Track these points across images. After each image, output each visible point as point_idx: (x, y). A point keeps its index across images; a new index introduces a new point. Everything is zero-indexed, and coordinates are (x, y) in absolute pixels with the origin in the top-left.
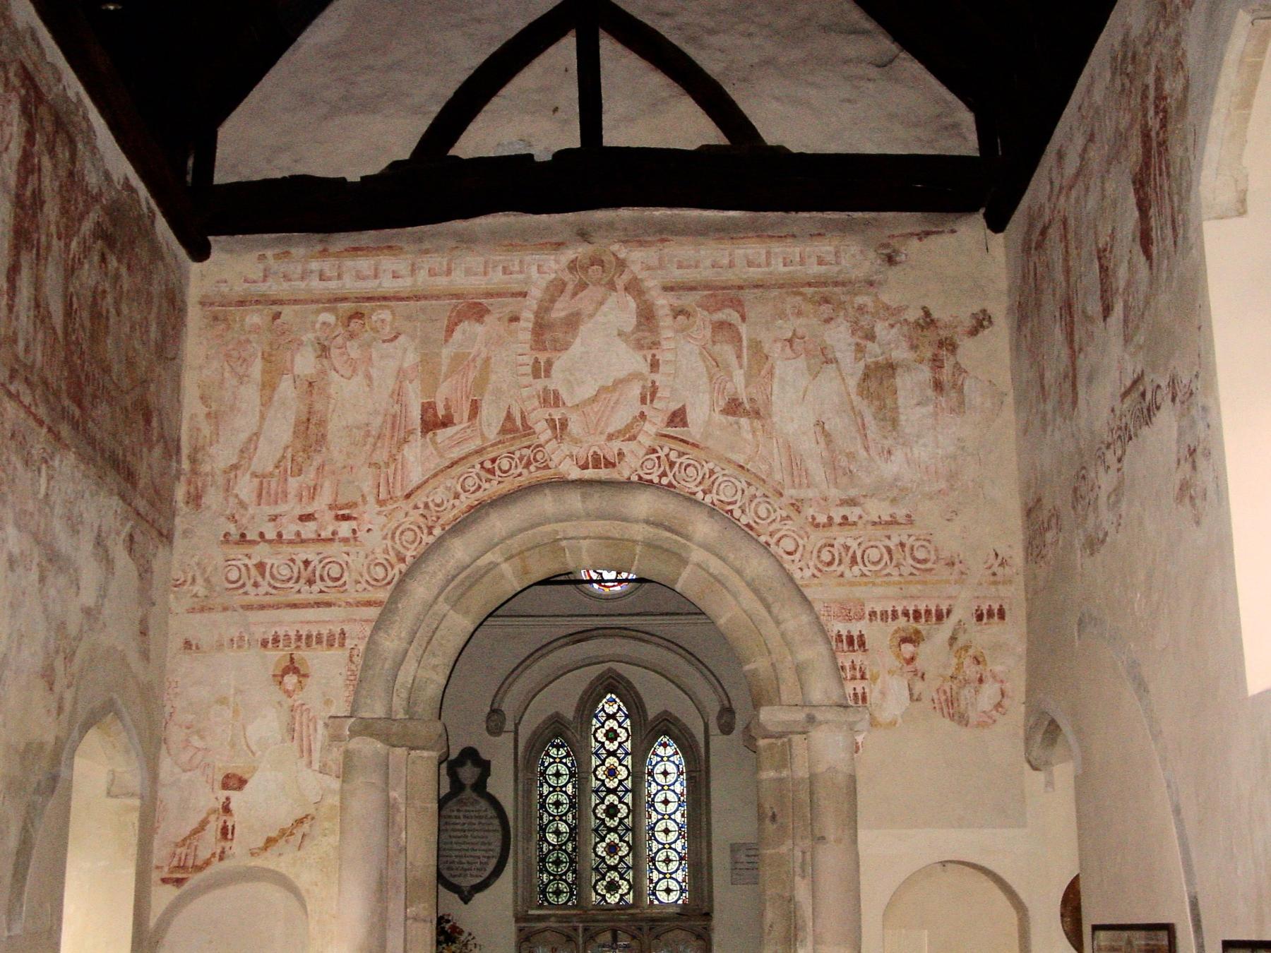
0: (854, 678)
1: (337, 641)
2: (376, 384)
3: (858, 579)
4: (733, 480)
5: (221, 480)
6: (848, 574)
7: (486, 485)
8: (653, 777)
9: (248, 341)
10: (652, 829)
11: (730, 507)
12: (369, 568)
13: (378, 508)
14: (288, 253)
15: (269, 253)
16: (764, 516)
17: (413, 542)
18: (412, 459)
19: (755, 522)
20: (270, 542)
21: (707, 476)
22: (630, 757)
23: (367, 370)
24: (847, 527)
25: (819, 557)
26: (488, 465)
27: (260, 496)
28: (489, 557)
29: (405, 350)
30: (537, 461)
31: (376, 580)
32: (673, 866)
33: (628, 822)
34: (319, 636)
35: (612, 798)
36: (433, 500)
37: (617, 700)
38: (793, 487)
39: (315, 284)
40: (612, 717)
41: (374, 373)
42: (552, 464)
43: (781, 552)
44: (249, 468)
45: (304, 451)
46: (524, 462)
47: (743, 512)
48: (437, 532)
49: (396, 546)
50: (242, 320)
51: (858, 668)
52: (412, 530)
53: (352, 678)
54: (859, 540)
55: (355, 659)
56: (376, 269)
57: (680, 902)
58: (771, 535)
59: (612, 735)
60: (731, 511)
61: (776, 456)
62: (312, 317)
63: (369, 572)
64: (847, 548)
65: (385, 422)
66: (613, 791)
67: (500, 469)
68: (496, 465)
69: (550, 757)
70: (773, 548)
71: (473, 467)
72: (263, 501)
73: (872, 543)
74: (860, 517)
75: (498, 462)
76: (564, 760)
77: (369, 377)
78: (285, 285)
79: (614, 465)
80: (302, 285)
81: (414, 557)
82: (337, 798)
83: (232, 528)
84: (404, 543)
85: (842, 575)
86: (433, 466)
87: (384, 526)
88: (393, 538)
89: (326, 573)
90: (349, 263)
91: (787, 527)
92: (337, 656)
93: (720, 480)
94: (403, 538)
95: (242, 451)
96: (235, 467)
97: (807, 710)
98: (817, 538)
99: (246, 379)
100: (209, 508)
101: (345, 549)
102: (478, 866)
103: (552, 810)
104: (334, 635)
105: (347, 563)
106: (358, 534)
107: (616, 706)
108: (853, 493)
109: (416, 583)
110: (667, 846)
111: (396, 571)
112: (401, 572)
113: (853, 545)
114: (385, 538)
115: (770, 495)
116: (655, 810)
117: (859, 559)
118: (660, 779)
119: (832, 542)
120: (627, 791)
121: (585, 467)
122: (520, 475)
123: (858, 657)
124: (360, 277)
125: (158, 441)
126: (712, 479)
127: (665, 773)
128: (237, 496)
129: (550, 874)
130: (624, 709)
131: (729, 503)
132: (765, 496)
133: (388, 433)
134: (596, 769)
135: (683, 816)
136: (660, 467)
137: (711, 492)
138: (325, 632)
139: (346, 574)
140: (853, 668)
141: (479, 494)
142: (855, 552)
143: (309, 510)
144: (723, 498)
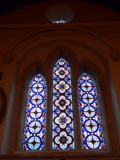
8: (81, 88)
10: (83, 110)
22: (70, 81)
32: (95, 128)
35: (62, 97)
40: (63, 66)
59: (62, 73)
66: (63, 94)
69: (36, 81)
76: (41, 82)
107: (64, 63)
118: (84, 89)
127: (87, 87)
129: (31, 133)
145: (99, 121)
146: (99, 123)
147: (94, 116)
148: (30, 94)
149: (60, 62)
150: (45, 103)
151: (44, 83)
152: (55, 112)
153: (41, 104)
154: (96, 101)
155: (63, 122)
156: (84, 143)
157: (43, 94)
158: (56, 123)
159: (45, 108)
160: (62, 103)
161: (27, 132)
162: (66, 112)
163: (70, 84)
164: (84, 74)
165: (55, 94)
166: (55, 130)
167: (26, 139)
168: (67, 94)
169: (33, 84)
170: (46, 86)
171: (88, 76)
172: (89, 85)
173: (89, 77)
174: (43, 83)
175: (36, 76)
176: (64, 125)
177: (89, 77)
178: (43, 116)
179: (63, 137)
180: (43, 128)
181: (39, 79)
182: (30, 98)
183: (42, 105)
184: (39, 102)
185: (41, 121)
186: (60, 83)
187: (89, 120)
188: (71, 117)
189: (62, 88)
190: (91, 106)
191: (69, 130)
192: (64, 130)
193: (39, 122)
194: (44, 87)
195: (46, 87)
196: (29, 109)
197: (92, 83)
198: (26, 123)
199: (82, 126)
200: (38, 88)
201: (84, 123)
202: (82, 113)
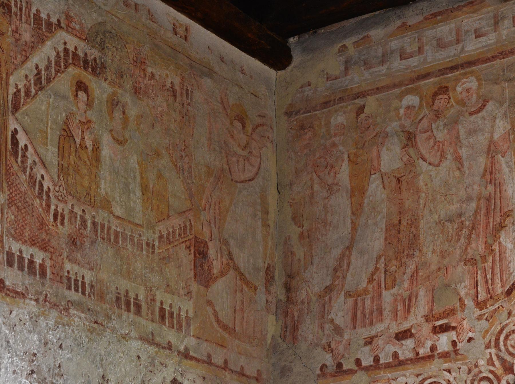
2: (466, 164)
5: (316, 307)
9: (334, 145)
13: (477, 312)
14: (367, 37)
15: (349, 42)
20: (367, 369)
23: (456, 151)
27: (354, 317)
29: (494, 119)
39: (397, 64)
41: (464, 152)
44: (343, 287)
45: (397, 258)
49: (501, 354)
50: (328, 124)
56: (457, 34)
62: (395, 103)
65: (478, 208)
72: (358, 323)
77: (458, 159)
78: (367, 74)
80: (383, 69)
83: (329, 360)
84: (511, 349)
87: (487, 332)
90: (430, 33)
94: (509, 342)
95: (335, 270)
96: (329, 289)
99: (335, 188)
100: (306, 339)
101: (446, 366)
106: (459, 345)
114: (488, 347)
124: (441, 45)
125: (223, 274)
128: (332, 320)
133: (482, 218)
143: (406, 326)
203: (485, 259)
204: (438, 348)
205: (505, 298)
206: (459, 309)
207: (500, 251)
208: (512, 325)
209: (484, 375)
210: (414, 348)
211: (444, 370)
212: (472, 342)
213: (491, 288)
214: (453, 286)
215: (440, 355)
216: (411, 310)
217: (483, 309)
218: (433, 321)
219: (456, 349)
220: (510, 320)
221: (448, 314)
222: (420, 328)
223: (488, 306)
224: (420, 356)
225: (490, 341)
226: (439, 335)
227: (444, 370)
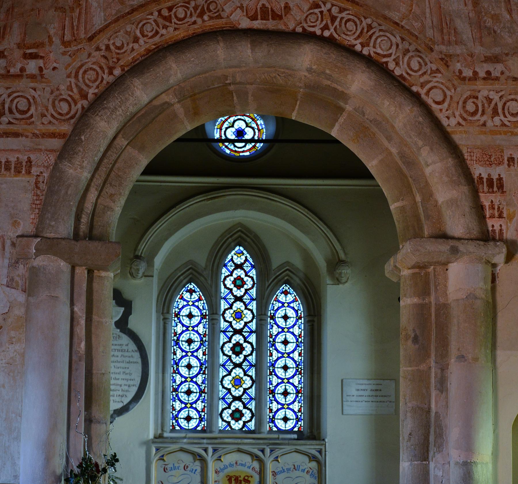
0: (492, 216)
1: (24, 169)
3: (499, 129)
4: (388, 35)
6: (490, 124)
7: (164, 31)
8: (274, 320)
10: (273, 365)
11: (385, 60)
12: (54, 103)
13: (63, 49)
16: (416, 68)
17: (95, 81)
18: (95, 4)
19: (408, 73)
21: (365, 30)
24: (490, 81)
25: (464, 107)
26: (165, 13)
28: (165, 98)
30: (210, 11)
31: (60, 114)
32: (290, 398)
33: (252, 359)
34: (8, 162)
35: (238, 338)
36: (114, 44)
37: (245, 252)
38: (443, 43)
42: (224, 15)
43: (430, 101)
46: (198, 11)
47: (397, 64)
48: (117, 72)
49: (79, 84)
51: (496, 207)
52: (94, 70)
53: (38, 202)
54: (500, 94)
55: (41, 185)
57: (296, 429)
58: (422, 86)
59: (239, 283)
60: (387, 63)
61: (428, 15)
63: (54, 106)
64: (489, 100)
66: (239, 332)
67: (176, 17)
68: (172, 13)
69: (185, 300)
70: (423, 96)
71: (152, 14)
73: (512, 97)
74: (502, 73)
75: (174, 10)
76: (196, 304)
79: (280, 17)
81: (95, 94)
82: (23, 310)
84: (87, 81)
85: (484, 125)
86: (114, 12)
87: (69, 65)
88: (76, 76)
89: (14, 105)
91: (435, 80)
92: (22, 179)
93: (377, 34)
94: (86, 76)
97: (452, 243)
98: (465, 90)
101: (32, 85)
102: (120, 393)
103: (185, 346)
104: (21, 163)
105: (34, 98)
106: (45, 71)
107: (243, 258)
108: (497, 50)
109: (98, 118)
110: (286, 381)
111: (79, 106)
112: (83, 108)
113: (496, 97)
114: (69, 76)
115: (422, 50)
116: (276, 349)
117: (500, 111)
119: (477, 94)
120: (251, 332)
121: (254, 18)
122: (195, 23)
123: (497, 198)
126: (370, 33)
127: (286, 318)
129: (182, 402)
130: (251, 260)
131: (385, 56)
132: (417, 50)
134: (224, 312)
135: (300, 355)
136: (322, 20)
137: (368, 45)
138: (13, 159)
139: (33, 110)
140: (492, 207)
141: (157, 39)
142: (496, 104)
144: (379, 51)
145: (300, 386)
146: (300, 388)
147: (293, 377)
148: (175, 328)
149: (235, 254)
150: (205, 348)
151: (203, 306)
152: (223, 366)
153: (197, 350)
154: (300, 349)
155: (237, 385)
156: (270, 421)
157: (201, 329)
158: (226, 386)
159: (205, 359)
160: (238, 349)
161: (175, 401)
162: (244, 367)
163: (255, 311)
164: (283, 288)
165: (224, 332)
166: (223, 398)
167: (174, 412)
168: (248, 332)
169: (180, 306)
170: (206, 313)
171: (291, 293)
172: (291, 313)
173: (293, 295)
174: (200, 304)
175: (186, 290)
176: (239, 391)
177: (293, 295)
178: (201, 372)
179: (237, 410)
180: (203, 395)
181: (193, 297)
182: (177, 338)
183: (200, 352)
184: (195, 347)
185: (199, 382)
186: (234, 308)
187: (282, 382)
188: (251, 377)
189: (238, 319)
190: (289, 357)
191: (248, 399)
192: (238, 399)
193: (196, 383)
194: (202, 314)
195: (206, 315)
196: (175, 360)
197: (298, 310)
198: (173, 386)
199: (270, 394)
200: (190, 316)
201: (273, 388)
202: (271, 370)
203: (73, 10)
204: (27, 70)
205: (86, 42)
206: (47, 43)
207: (86, 6)
208: (90, 64)
209: (64, 97)
210: (6, 67)
211: (30, 88)
212: (56, 71)
213: (75, 32)
214: (44, 25)
215: (28, 76)
216: (5, 37)
217: (68, 47)
218: (24, 48)
219: (42, 73)
220: (89, 60)
221: (38, 46)
222: (12, 52)
223: (72, 46)
224: (11, 74)
225: (71, 73)
226: (29, 61)
227: (30, 88)
